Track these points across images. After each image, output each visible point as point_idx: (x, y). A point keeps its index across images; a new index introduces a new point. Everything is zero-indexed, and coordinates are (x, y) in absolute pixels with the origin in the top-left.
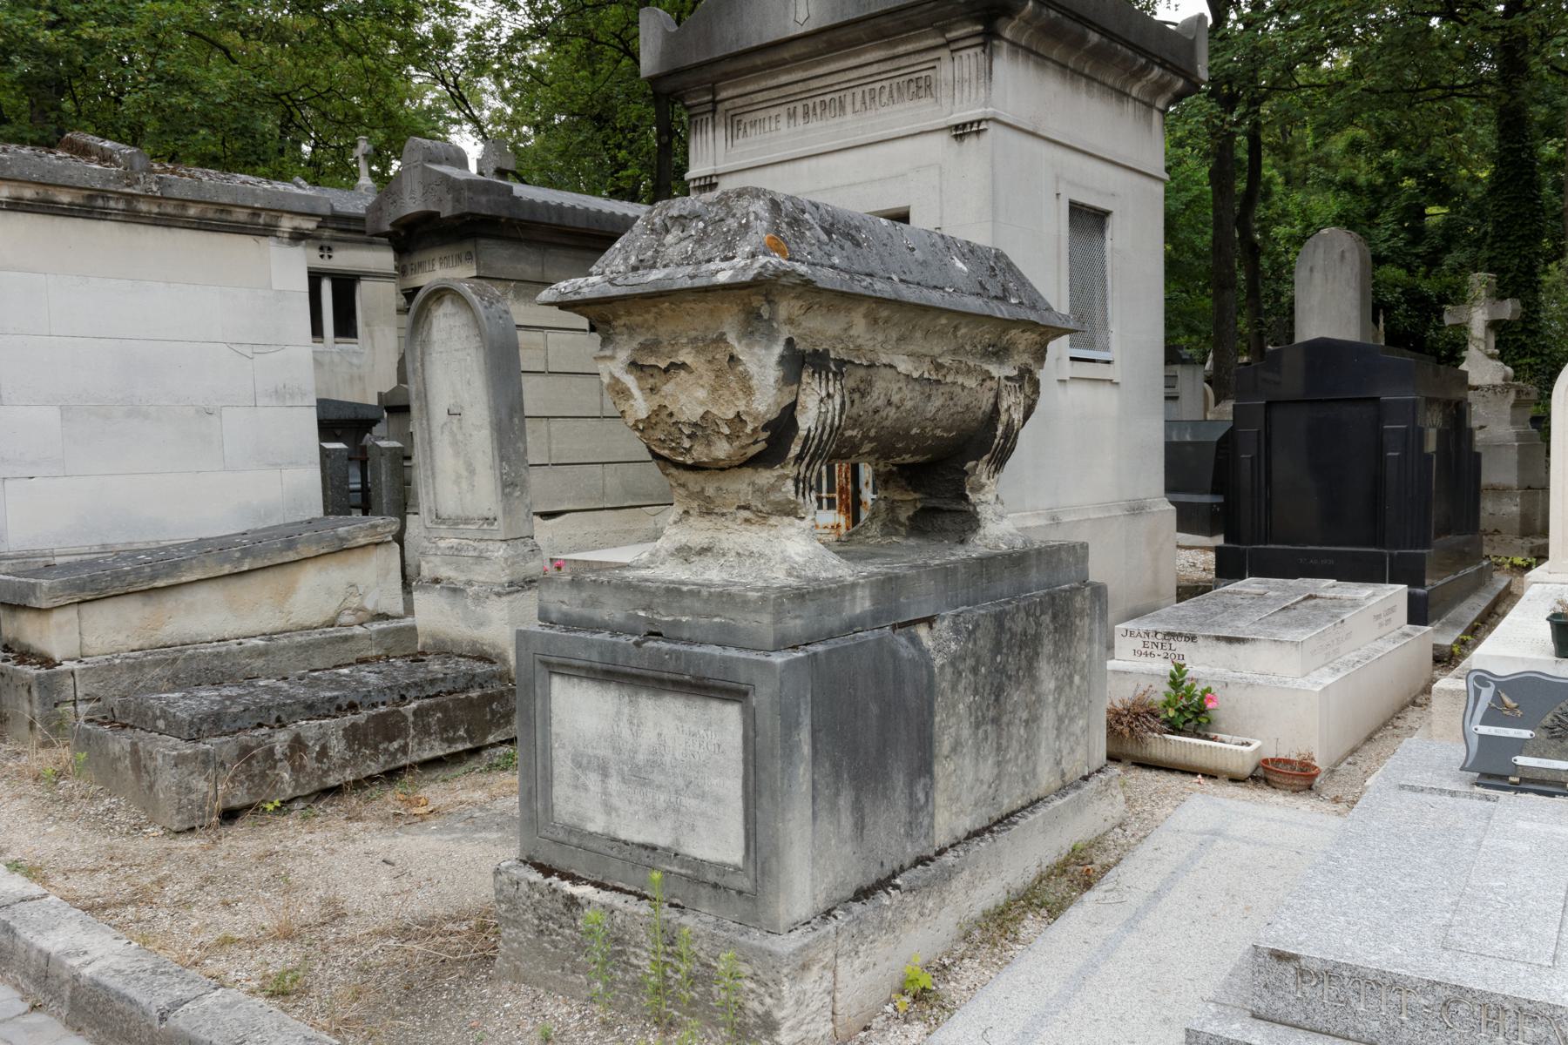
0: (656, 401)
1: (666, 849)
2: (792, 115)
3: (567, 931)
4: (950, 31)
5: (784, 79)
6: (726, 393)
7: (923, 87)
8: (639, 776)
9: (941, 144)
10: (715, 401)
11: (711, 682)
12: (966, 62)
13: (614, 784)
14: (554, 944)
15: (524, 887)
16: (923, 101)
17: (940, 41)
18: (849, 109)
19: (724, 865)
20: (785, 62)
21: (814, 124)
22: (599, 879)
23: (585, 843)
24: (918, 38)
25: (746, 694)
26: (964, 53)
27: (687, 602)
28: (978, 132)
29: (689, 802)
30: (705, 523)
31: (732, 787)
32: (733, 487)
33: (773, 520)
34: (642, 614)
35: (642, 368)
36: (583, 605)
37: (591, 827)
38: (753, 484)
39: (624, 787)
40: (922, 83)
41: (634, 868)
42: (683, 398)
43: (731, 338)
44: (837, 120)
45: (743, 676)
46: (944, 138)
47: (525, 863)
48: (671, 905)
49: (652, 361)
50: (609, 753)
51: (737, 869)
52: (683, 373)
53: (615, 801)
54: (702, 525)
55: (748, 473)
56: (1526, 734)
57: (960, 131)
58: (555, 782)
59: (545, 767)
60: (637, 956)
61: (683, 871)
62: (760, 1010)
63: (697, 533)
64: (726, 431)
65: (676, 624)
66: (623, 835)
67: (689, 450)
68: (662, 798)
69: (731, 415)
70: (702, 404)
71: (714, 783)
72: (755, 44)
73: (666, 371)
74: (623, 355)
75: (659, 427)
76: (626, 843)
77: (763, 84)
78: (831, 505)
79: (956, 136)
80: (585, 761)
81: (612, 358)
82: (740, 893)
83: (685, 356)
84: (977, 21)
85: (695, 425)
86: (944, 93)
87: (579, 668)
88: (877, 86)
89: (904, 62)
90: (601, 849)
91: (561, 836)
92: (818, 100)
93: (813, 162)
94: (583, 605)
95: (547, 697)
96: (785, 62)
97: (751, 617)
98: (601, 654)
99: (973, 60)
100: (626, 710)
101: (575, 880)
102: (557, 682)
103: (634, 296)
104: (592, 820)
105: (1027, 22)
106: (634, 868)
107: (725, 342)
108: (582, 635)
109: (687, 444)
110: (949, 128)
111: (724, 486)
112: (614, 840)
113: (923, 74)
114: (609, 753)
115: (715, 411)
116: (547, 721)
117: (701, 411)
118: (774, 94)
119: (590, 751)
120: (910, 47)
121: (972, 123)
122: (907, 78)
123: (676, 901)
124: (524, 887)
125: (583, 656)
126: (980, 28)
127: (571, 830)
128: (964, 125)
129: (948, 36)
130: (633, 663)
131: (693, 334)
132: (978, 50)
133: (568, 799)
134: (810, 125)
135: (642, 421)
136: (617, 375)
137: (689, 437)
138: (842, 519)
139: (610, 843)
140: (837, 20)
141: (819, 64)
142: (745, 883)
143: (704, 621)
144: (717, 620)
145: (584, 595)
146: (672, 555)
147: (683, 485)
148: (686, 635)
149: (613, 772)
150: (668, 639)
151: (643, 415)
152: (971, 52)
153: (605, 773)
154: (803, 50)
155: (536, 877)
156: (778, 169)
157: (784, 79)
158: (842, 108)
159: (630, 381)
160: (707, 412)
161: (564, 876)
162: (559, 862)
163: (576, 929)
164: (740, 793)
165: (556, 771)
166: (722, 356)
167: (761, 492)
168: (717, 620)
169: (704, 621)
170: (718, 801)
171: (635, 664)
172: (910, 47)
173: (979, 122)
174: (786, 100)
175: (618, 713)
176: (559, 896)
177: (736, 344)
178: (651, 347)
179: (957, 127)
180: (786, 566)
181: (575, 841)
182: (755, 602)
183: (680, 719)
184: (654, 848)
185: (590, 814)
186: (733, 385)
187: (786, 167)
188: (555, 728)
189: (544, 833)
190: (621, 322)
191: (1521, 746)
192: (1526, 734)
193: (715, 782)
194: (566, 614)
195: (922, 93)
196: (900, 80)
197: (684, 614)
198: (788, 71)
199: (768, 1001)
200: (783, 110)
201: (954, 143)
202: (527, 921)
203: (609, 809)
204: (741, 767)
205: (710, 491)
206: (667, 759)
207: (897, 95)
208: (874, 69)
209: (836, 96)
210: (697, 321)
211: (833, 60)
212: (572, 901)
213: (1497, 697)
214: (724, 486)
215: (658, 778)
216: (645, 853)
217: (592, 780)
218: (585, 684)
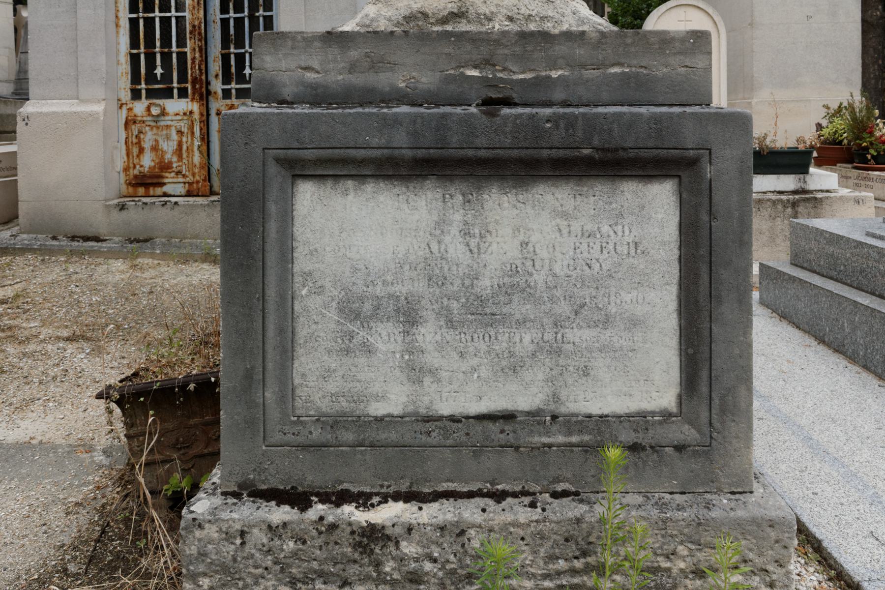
8: (481, 312)
11: (632, 154)
13: (428, 334)
15: (259, 536)
19: (643, 415)
22: (404, 487)
23: (371, 435)
25: (692, 163)
27: (561, 49)
29: (579, 335)
31: (661, 303)
34: (475, 73)
36: (352, 68)
37: (378, 409)
41: (476, 455)
45: (690, 138)
47: (237, 495)
48: (555, 495)
50: (420, 287)
51: (666, 415)
53: (432, 359)
58: (300, 351)
59: (281, 331)
61: (575, 439)
65: (541, 83)
66: (445, 409)
68: (527, 339)
71: (627, 299)
76: (453, 419)
80: (367, 307)
82: (679, 448)
90: (408, 438)
91: (317, 434)
94: (352, 68)
95: (287, 216)
97: (674, 61)
100: (457, 217)
101: (363, 500)
102: (307, 195)
104: (380, 397)
106: (476, 455)
112: (428, 419)
114: (420, 287)
116: (287, 256)
119: (379, 290)
123: (560, 487)
124: (259, 536)
125: (375, 142)
127: (335, 422)
130: (481, 141)
133: (327, 374)
139: (420, 426)
142: (687, 433)
143: (589, 74)
145: (354, 54)
148: (559, 95)
149: (429, 315)
150: (526, 105)
153: (408, 316)
155: (281, 514)
161: (341, 498)
162: (311, 476)
164: (673, 305)
165: (302, 331)
169: (589, 74)
170: (634, 323)
175: (442, 223)
176: (343, 534)
181: (349, 436)
183: (565, 215)
184: (508, 417)
185: (377, 388)
188: (302, 263)
189: (278, 437)
193: (627, 297)
194: (314, 86)
197: (555, 67)
203: (416, 372)
206: (539, 278)
212: (373, 535)
215: (519, 308)
216: (493, 428)
217: (386, 338)
218: (369, 187)
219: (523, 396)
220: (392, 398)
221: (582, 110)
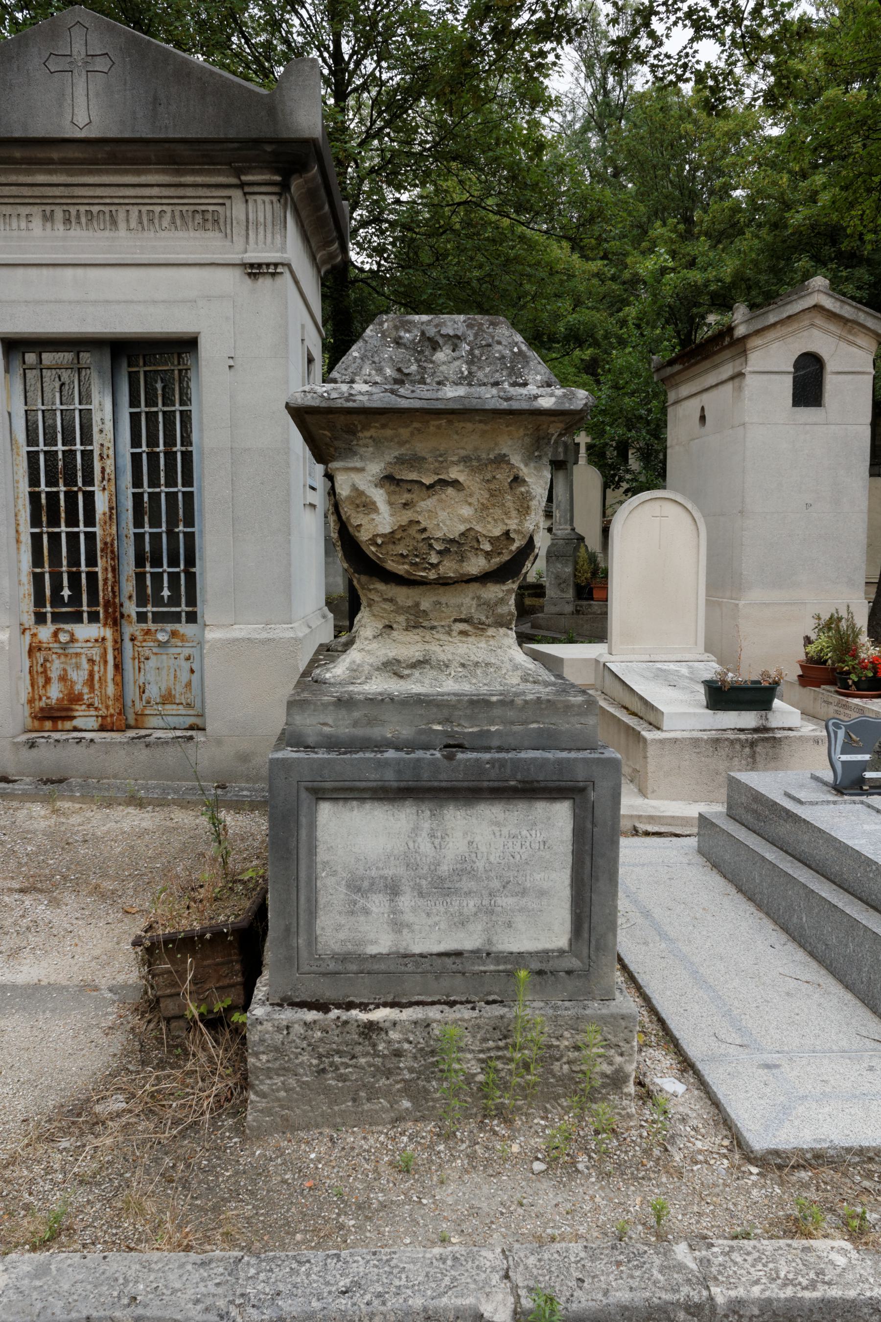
0: (406, 516)
1: (476, 952)
2: (48, 218)
3: (362, 1061)
4: (245, 174)
5: (41, 178)
6: (498, 512)
7: (210, 221)
8: (440, 887)
9: (231, 279)
10: (481, 519)
11: (542, 784)
12: (261, 207)
13: (406, 901)
14: (343, 1078)
15: (298, 1029)
16: (210, 234)
17: (233, 180)
18: (122, 225)
19: (546, 952)
20: (51, 162)
21: (76, 232)
22: (389, 999)
23: (368, 966)
24: (209, 173)
25: (582, 790)
26: (259, 198)
27: (497, 712)
28: (273, 275)
29: (506, 901)
30: (413, 636)
31: (560, 881)
32: (453, 601)
33: (491, 632)
34: (439, 727)
35: (398, 482)
36: (355, 724)
37: (372, 950)
38: (479, 598)
39: (421, 902)
40: (209, 216)
41: (437, 978)
42: (443, 515)
43: (516, 460)
44: (107, 233)
45: (581, 774)
46: (237, 273)
47: (280, 1005)
48: (488, 1003)
49: (413, 476)
50: (401, 871)
51: (561, 952)
52: (450, 491)
53: (409, 917)
54: (408, 639)
55: (475, 586)
56: (867, 757)
57: (255, 271)
58: (320, 913)
59: (309, 900)
60: (459, 1060)
61: (501, 968)
62: (607, 1069)
63: (407, 646)
64: (487, 547)
65: (483, 734)
66: (417, 949)
67: (434, 566)
68: (471, 904)
69: (497, 532)
70: (464, 520)
71: (537, 878)
72: (17, 135)
73: (430, 487)
74: (375, 468)
75: (403, 543)
76: (422, 956)
77: (13, 178)
78: (94, 618)
79: (249, 274)
80: (366, 884)
81: (361, 470)
82: (569, 973)
83: (454, 473)
84: (277, 171)
85: (452, 541)
86: (238, 231)
87: (364, 790)
88: (158, 209)
89: (190, 192)
90: (392, 968)
91: (332, 966)
92: (83, 209)
93: (80, 271)
94: (355, 724)
95: (313, 825)
96: (51, 162)
97: (574, 720)
98: (399, 772)
99: (268, 207)
100: (426, 825)
101: (363, 1007)
102: (325, 810)
103: (416, 410)
104: (372, 942)
105: (306, 182)
106: (437, 978)
107: (508, 463)
108: (360, 755)
109: (434, 559)
110: (244, 265)
111: (443, 600)
112: (405, 956)
113: (211, 208)
114: (401, 871)
115: (478, 528)
116: (312, 850)
117: (462, 528)
118: (26, 191)
119: (374, 873)
120: (199, 179)
121: (268, 265)
122: (192, 208)
123: (491, 998)
124: (298, 1029)
125: (372, 777)
126: (278, 178)
127: (344, 958)
128: (260, 265)
129: (244, 178)
130: (443, 776)
131: (463, 453)
132: (274, 198)
133: (338, 928)
134: (72, 233)
135: (383, 536)
136: (362, 487)
137: (439, 552)
138: (108, 633)
139: (401, 960)
140: (127, 135)
141: (90, 172)
142: (574, 963)
143: (517, 728)
144: (535, 726)
145: (356, 714)
146: (378, 669)
147: (391, 600)
148: (495, 743)
149: (406, 889)
150: (473, 749)
151: (387, 530)
152: (267, 198)
153: (393, 889)
154: (77, 155)
155: (311, 1016)
156: (33, 272)
157: (41, 178)
158: (114, 222)
159: (379, 496)
160: (471, 529)
161: (350, 1006)
162: (328, 993)
163: (376, 1054)
164: (567, 881)
165: (322, 900)
166: (503, 477)
167: (483, 604)
168: (535, 726)
169: (517, 728)
170: (542, 893)
171: (444, 778)
172: (199, 179)
173: (276, 265)
174: (41, 201)
175: (416, 829)
176: (353, 1027)
177: (522, 466)
178: (415, 461)
179: (252, 265)
180: (519, 673)
181: (354, 967)
182: (580, 706)
183: (498, 824)
184: (458, 954)
185: (372, 936)
186: (509, 504)
187: (45, 271)
188: (322, 855)
189: (306, 968)
190: (367, 434)
191: (864, 766)
192: (867, 757)
193: (538, 877)
194: (329, 737)
195: (209, 225)
196: (185, 208)
197: (492, 723)
198: (50, 172)
199: (618, 1059)
200: (36, 210)
201: (248, 281)
202: (301, 1064)
203: (398, 925)
204: (569, 859)
205: (425, 605)
206: (480, 865)
207: (182, 221)
208: (155, 191)
209: (106, 209)
210: (469, 440)
211: (107, 172)
213: (847, 735)
214: (443, 600)
215: (466, 884)
216: (448, 961)
217: (378, 904)
218: (368, 806)
219: (468, 940)
220: (381, 942)
221: (510, 755)
